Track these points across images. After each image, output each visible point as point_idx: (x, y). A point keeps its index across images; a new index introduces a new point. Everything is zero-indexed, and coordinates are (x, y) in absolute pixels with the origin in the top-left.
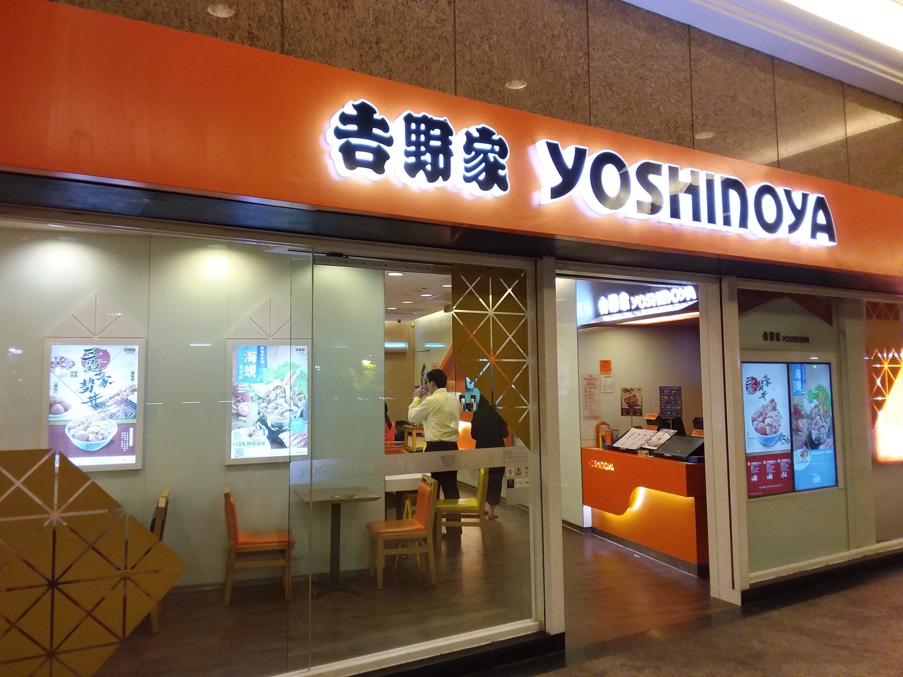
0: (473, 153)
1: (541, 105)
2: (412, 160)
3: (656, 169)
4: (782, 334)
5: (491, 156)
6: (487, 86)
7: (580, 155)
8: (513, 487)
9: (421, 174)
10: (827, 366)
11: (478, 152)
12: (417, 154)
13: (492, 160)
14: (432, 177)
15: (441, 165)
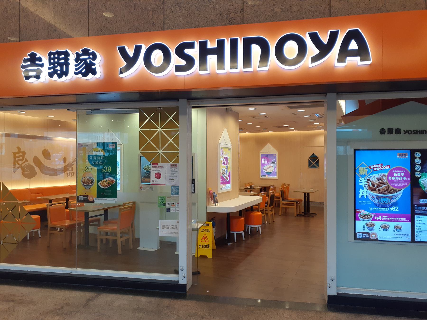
0: (79, 61)
1: (134, 28)
2: (52, 70)
3: (191, 45)
4: (402, 129)
5: (88, 61)
6: (104, 27)
7: (138, 50)
8: (170, 211)
9: (56, 76)
10: (357, 152)
11: (82, 60)
12: (54, 68)
13: (89, 62)
14: (60, 76)
15: (64, 70)
